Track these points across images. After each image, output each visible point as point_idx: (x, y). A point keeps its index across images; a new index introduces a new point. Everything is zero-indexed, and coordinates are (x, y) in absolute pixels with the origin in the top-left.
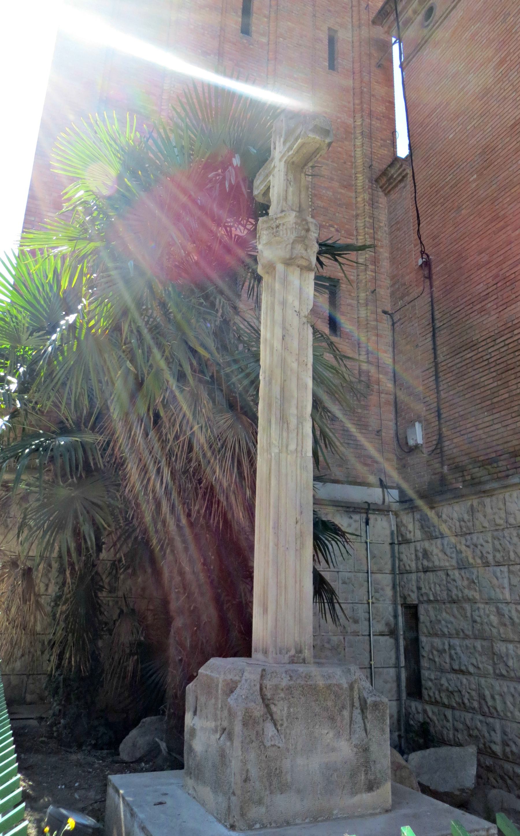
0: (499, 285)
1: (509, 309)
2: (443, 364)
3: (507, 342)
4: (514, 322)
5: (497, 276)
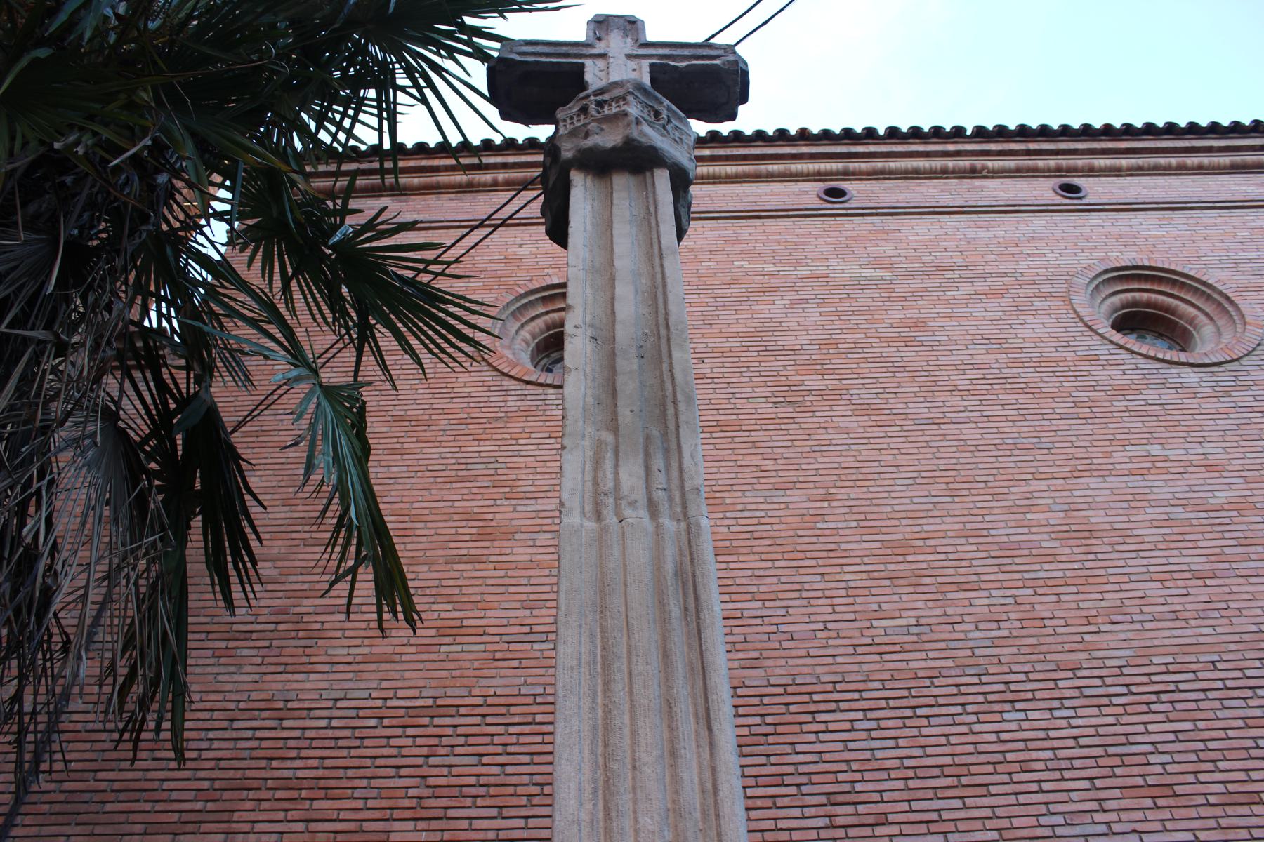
0: (281, 627)
1: (285, 677)
2: (75, 717)
3: (259, 734)
4: (290, 705)
5: (283, 611)
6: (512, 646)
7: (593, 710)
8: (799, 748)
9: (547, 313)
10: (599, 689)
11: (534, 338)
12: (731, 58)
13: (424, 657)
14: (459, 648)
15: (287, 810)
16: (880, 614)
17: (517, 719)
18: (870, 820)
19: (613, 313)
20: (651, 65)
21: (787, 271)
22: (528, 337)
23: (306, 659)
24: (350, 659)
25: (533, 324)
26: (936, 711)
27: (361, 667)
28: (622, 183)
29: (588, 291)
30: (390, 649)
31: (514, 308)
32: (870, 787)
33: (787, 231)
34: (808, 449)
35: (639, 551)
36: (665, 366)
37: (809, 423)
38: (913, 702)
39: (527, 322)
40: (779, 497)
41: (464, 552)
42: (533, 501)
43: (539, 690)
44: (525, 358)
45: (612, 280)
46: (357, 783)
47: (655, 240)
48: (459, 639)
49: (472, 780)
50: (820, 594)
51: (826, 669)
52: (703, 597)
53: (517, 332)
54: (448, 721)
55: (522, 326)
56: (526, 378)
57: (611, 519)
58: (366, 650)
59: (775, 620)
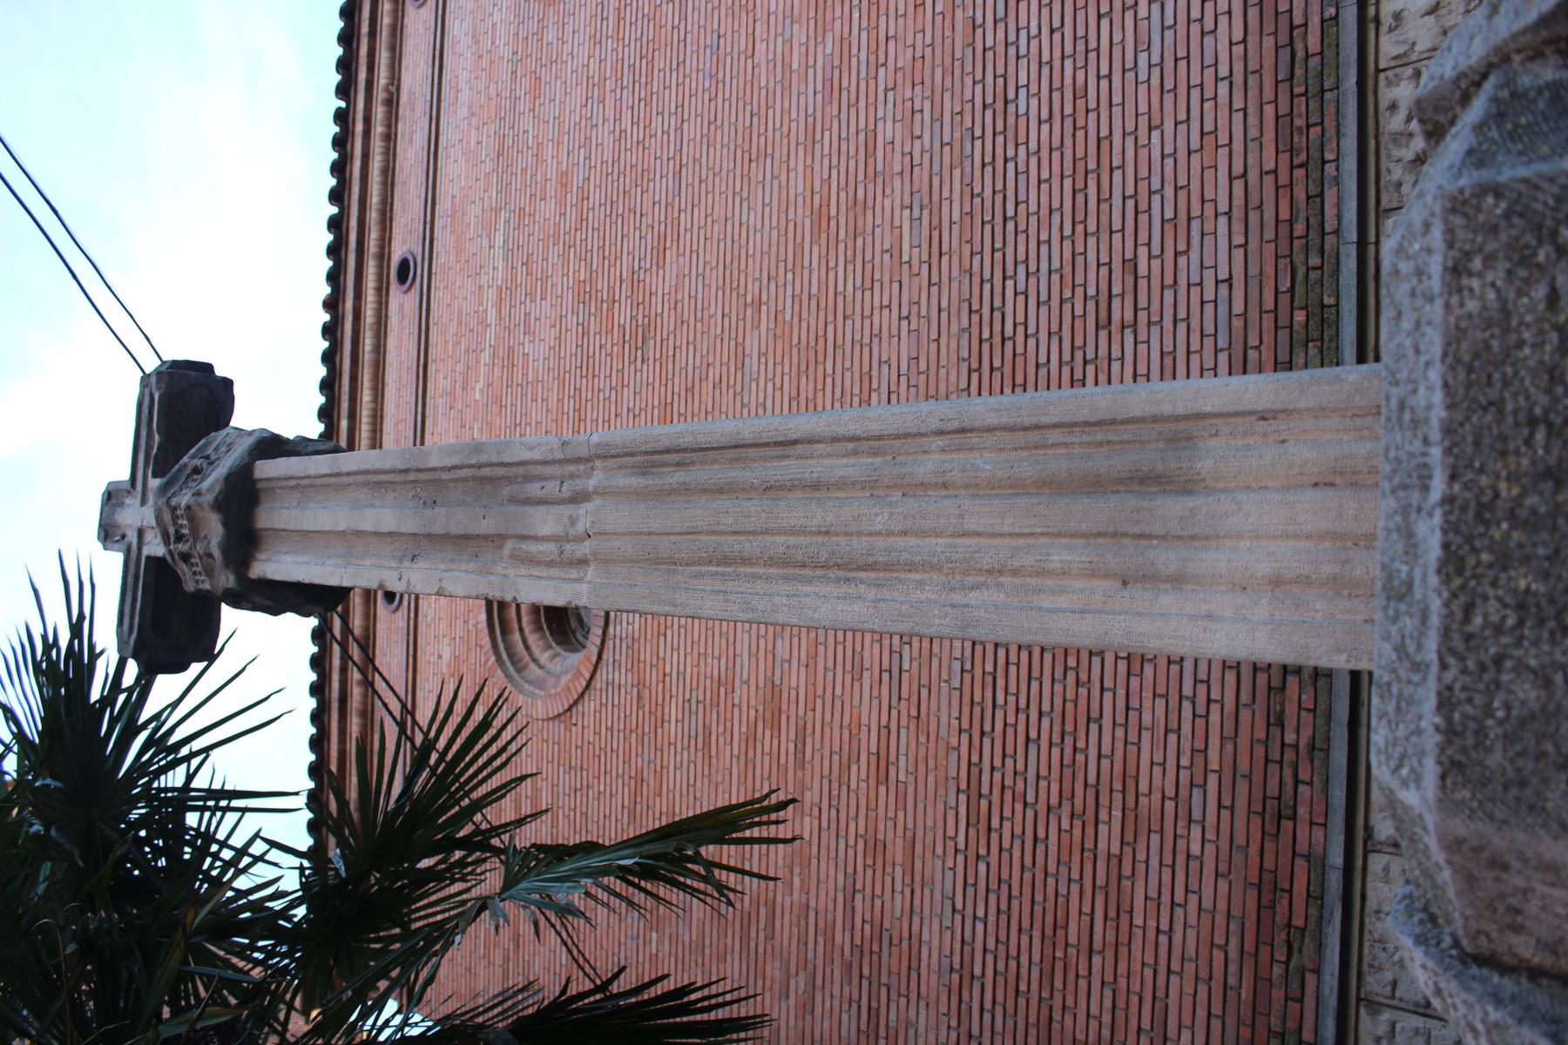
0: (866, 971)
1: (924, 971)
3: (988, 1005)
4: (957, 966)
5: (847, 968)
6: (905, 694)
7: (768, 578)
8: (1043, 359)
9: (521, 630)
10: (750, 570)
11: (550, 647)
12: (154, 379)
13: (910, 801)
14: (902, 759)
15: (1077, 976)
16: (895, 251)
17: (989, 695)
18: (1130, 279)
19: (389, 534)
20: (155, 476)
21: (490, 336)
22: (548, 654)
23: (905, 944)
24: (907, 891)
25: (533, 647)
26: (1010, 194)
27: (918, 878)
28: (269, 516)
29: (368, 562)
30: (899, 841)
31: (511, 669)
32: (1092, 277)
33: (444, 333)
34: (699, 325)
35: (620, 516)
36: (445, 476)
37: (669, 322)
38: (999, 219)
39: (531, 655)
40: (752, 363)
41: (791, 747)
42: (738, 660)
43: (957, 665)
44: (573, 659)
45: (358, 533)
46: (1050, 890)
47: (324, 481)
48: (892, 759)
49: (1056, 751)
50: (867, 322)
51: (954, 319)
52: (666, 443)
53: (541, 667)
54: (986, 777)
55: (534, 660)
56: (594, 659)
57: (585, 549)
58: (899, 871)
59: (894, 377)
